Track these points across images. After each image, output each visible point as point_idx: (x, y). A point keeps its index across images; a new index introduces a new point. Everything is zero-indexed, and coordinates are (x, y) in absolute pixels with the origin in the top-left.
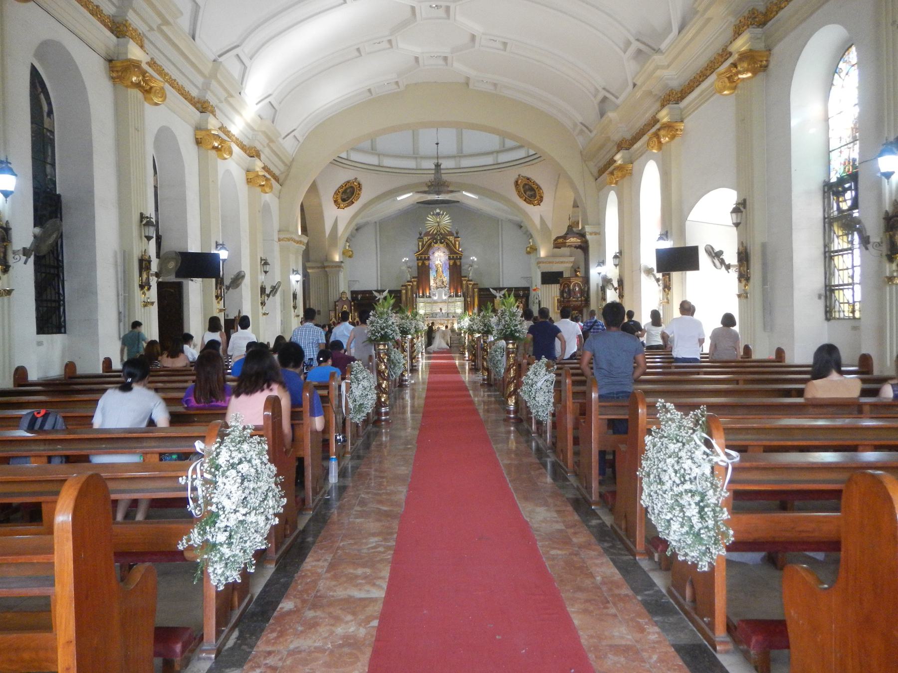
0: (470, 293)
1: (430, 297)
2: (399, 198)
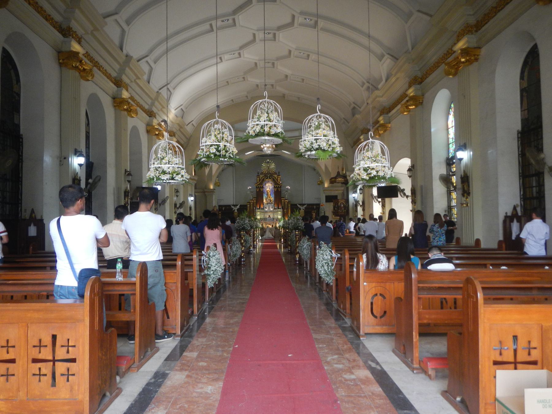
0: (286, 207)
1: (263, 209)
2: (246, 154)
